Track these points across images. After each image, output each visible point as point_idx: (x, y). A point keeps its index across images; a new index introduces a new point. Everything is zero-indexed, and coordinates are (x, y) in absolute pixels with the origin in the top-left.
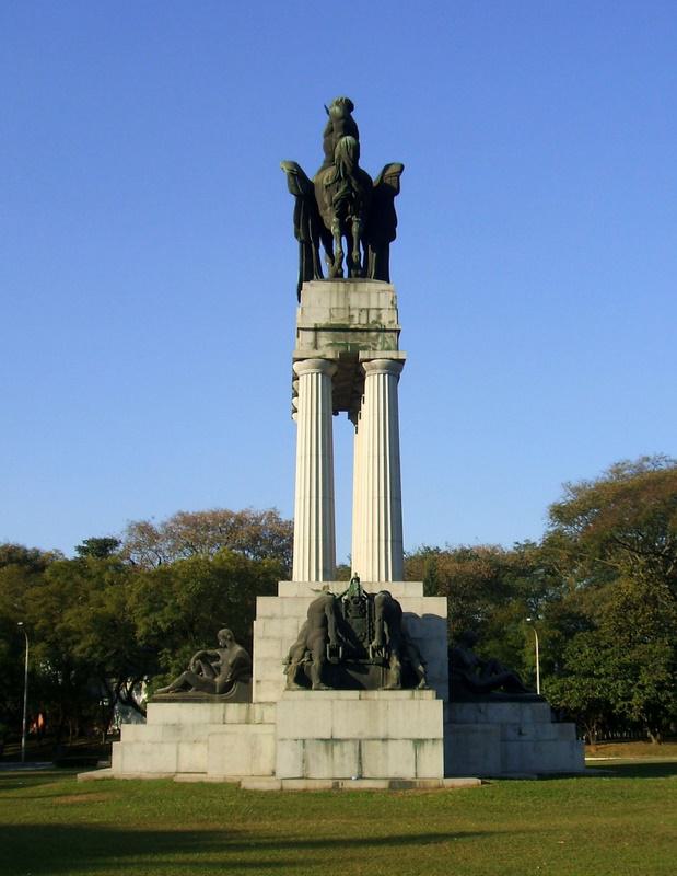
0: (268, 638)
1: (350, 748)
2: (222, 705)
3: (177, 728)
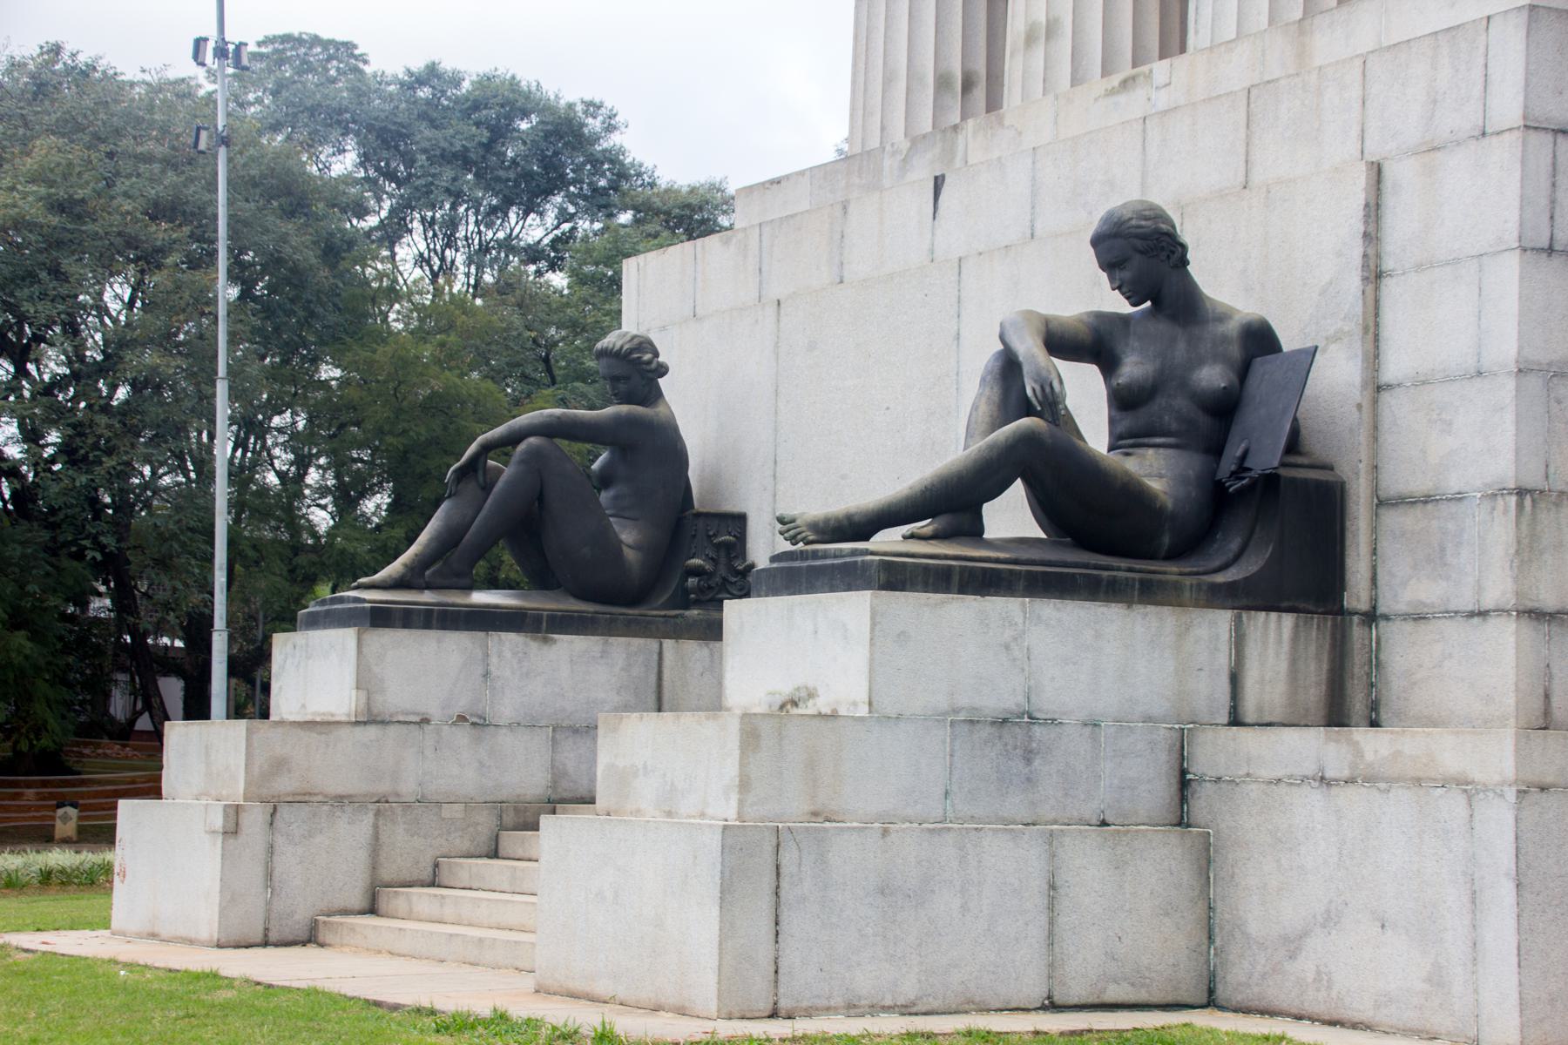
2: (1221, 621)
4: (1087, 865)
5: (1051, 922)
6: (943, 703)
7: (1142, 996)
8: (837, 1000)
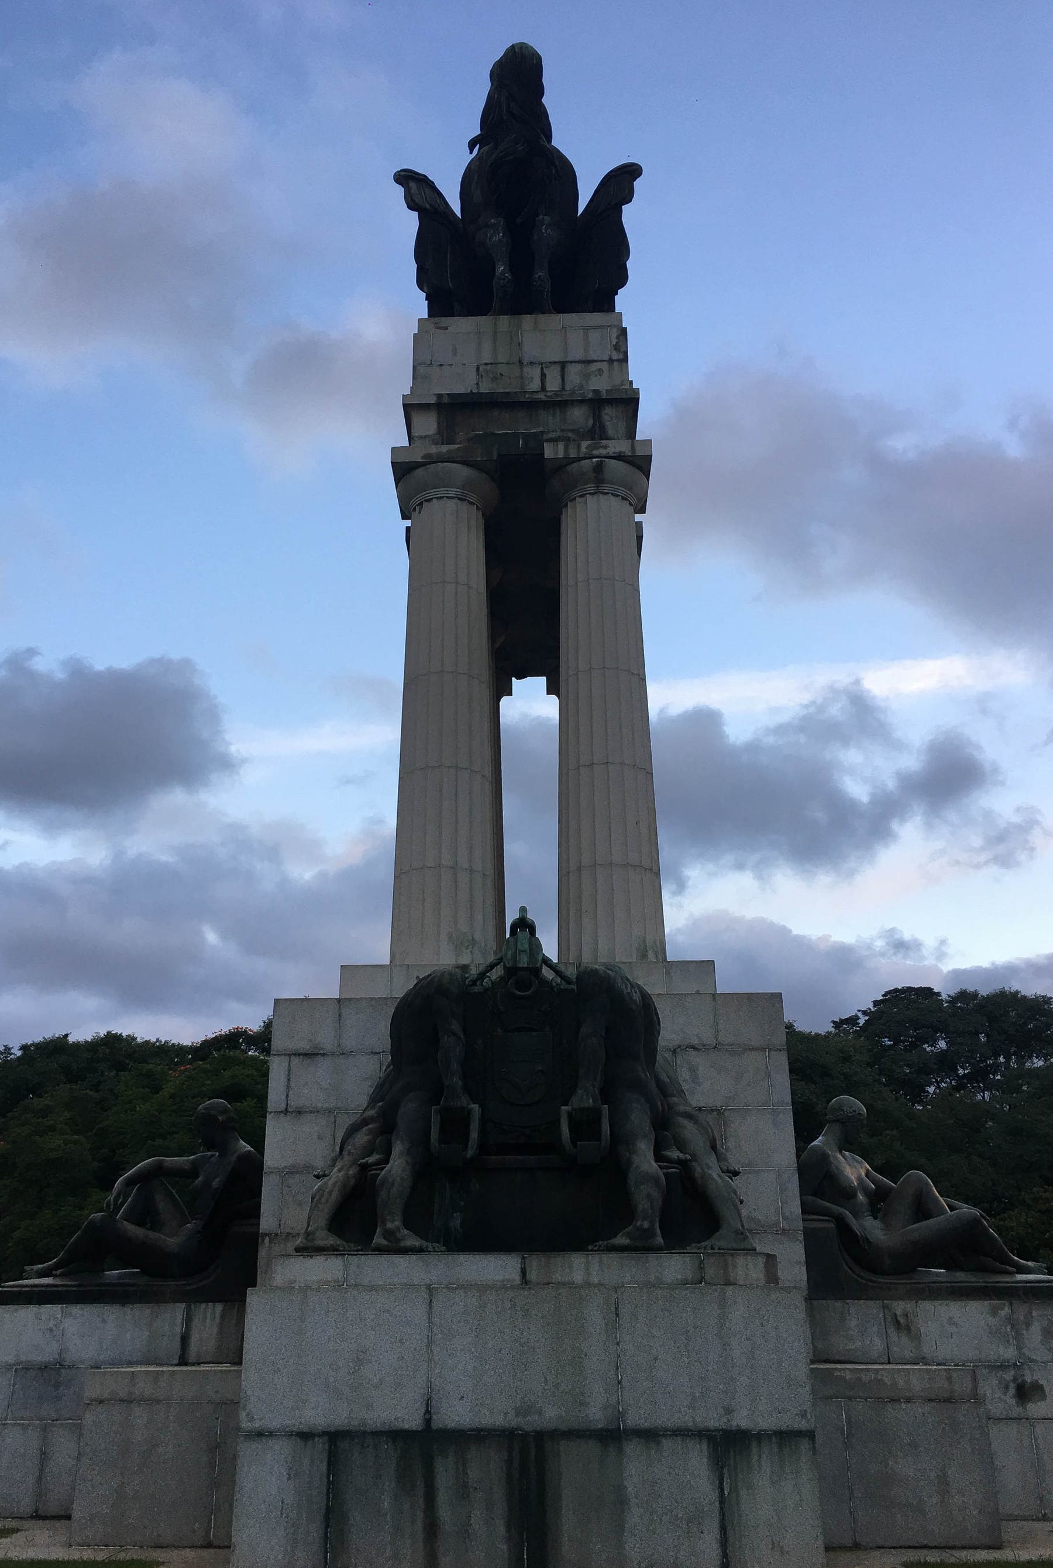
0: (299, 1112)
1: (486, 1470)
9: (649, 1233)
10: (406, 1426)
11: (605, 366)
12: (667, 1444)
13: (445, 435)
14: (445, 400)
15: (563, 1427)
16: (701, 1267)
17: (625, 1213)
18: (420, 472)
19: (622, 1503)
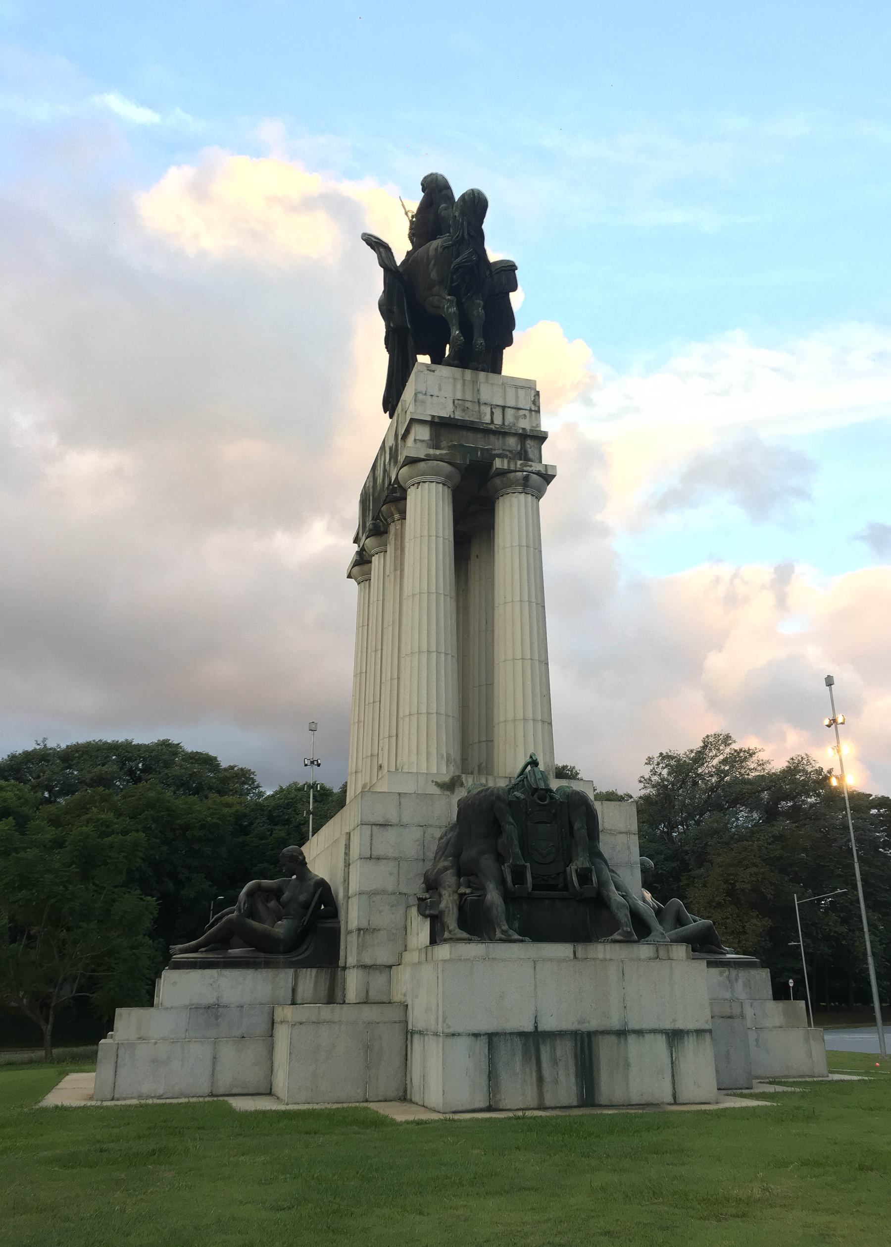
0: (378, 859)
1: (565, 1050)
2: (290, 972)
3: (212, 1011)
4: (228, 1052)
5: (214, 1069)
6: (187, 1002)
7: (246, 1091)
8: (135, 1095)
9: (629, 934)
10: (526, 1030)
11: (527, 413)
12: (648, 1036)
13: (435, 443)
14: (436, 420)
15: (599, 1029)
16: (657, 951)
17: (614, 925)
18: (422, 464)
19: (627, 1065)
